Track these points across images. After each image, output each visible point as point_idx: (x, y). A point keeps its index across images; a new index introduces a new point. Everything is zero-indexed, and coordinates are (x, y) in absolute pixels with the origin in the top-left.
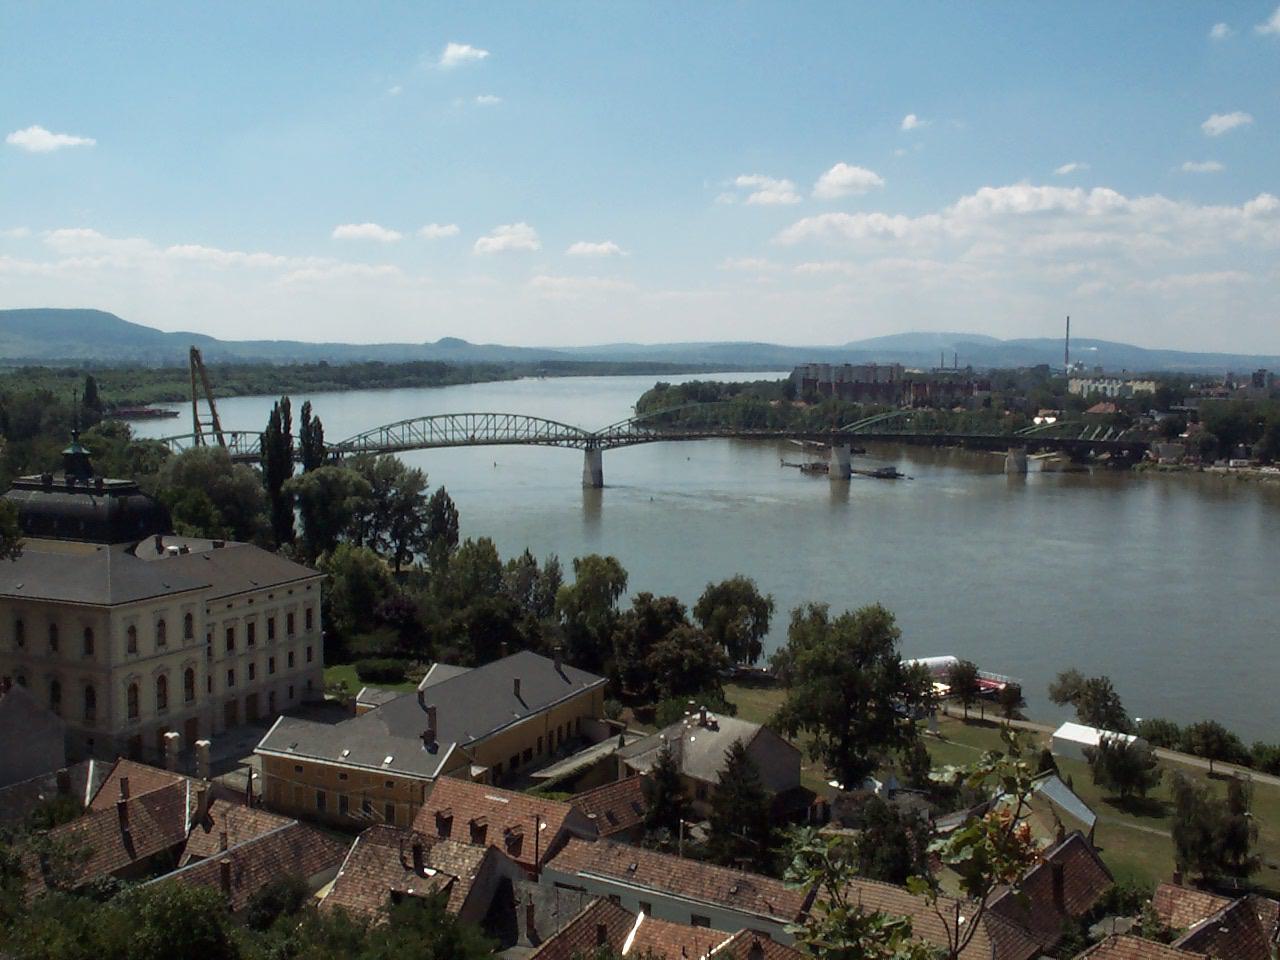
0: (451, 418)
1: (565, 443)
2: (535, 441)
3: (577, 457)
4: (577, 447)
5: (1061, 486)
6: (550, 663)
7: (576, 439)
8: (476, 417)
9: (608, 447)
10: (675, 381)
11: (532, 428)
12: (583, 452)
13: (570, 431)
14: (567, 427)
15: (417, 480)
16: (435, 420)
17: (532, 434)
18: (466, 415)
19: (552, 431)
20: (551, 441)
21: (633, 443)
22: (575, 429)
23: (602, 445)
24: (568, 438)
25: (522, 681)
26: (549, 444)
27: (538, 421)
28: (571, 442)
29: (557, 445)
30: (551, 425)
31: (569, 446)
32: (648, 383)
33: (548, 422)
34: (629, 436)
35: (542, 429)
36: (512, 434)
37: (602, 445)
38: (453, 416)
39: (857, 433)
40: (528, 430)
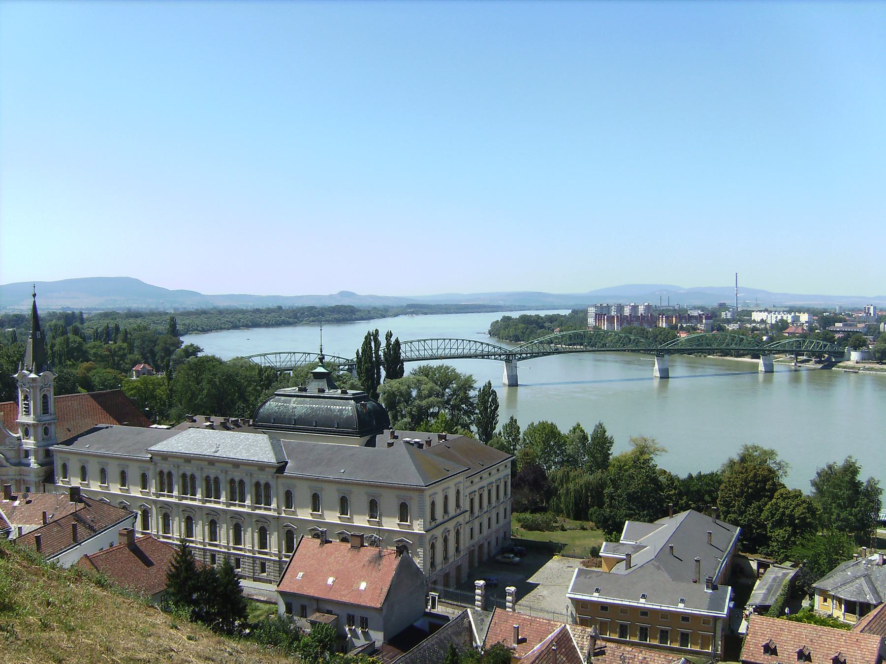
0: (409, 344)
1: (493, 357)
2: (476, 356)
4: (501, 360)
9: (520, 359)
10: (515, 315)
13: (496, 349)
15: (467, 384)
16: (426, 341)
17: (472, 352)
18: (432, 340)
21: (535, 357)
26: (483, 358)
27: (477, 343)
28: (497, 356)
29: (489, 359)
31: (495, 359)
32: (498, 316)
33: (482, 343)
36: (460, 351)
37: (517, 357)
38: (425, 341)
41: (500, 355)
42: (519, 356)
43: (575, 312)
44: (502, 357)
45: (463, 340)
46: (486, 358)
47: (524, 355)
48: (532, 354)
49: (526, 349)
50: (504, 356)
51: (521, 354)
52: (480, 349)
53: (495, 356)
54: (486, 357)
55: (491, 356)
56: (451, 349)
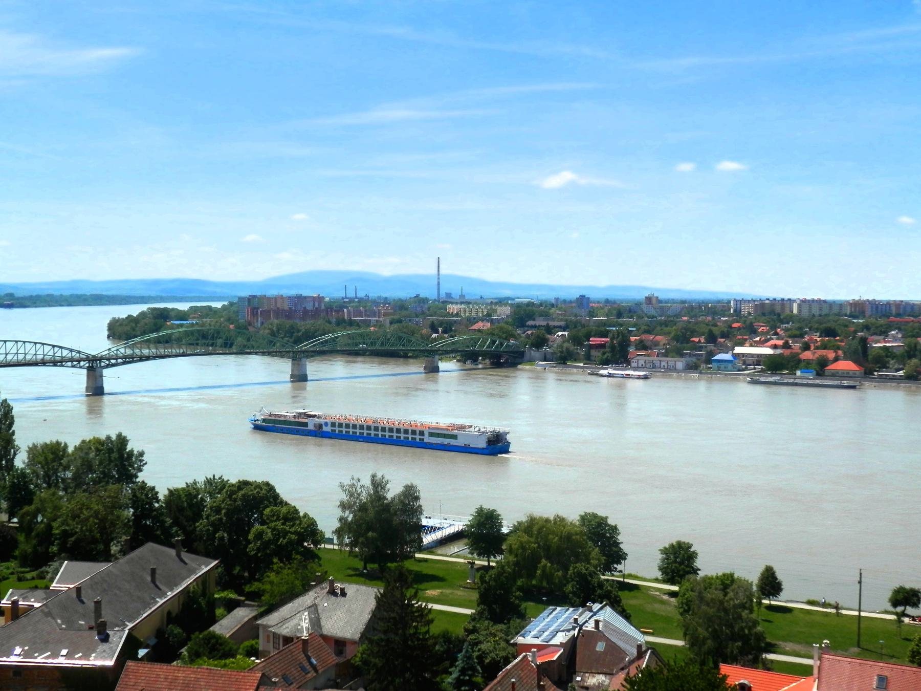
1: (69, 364)
2: (43, 363)
3: (78, 378)
4: (81, 367)
5: (397, 394)
6: (173, 552)
7: (79, 361)
8: (7, 343)
9: (107, 366)
11: (40, 352)
12: (85, 372)
13: (74, 354)
14: (71, 350)
17: (40, 357)
19: (59, 354)
20: (55, 363)
22: (79, 352)
23: (103, 364)
24: (72, 360)
25: (158, 572)
28: (75, 363)
29: (63, 366)
30: (56, 349)
31: (73, 366)
33: (54, 346)
34: (125, 357)
35: (49, 352)
36: (21, 357)
37: (103, 364)
39: (312, 349)
40: (36, 354)
41: (79, 361)
42: (107, 362)
43: (231, 304)
44: (82, 363)
45: (24, 342)
46: (59, 366)
47: (113, 361)
48: (126, 359)
49: (115, 352)
50: (85, 363)
51: (109, 360)
52: (51, 353)
53: (72, 362)
54: (59, 364)
55: (67, 362)
56: (17, 353)
